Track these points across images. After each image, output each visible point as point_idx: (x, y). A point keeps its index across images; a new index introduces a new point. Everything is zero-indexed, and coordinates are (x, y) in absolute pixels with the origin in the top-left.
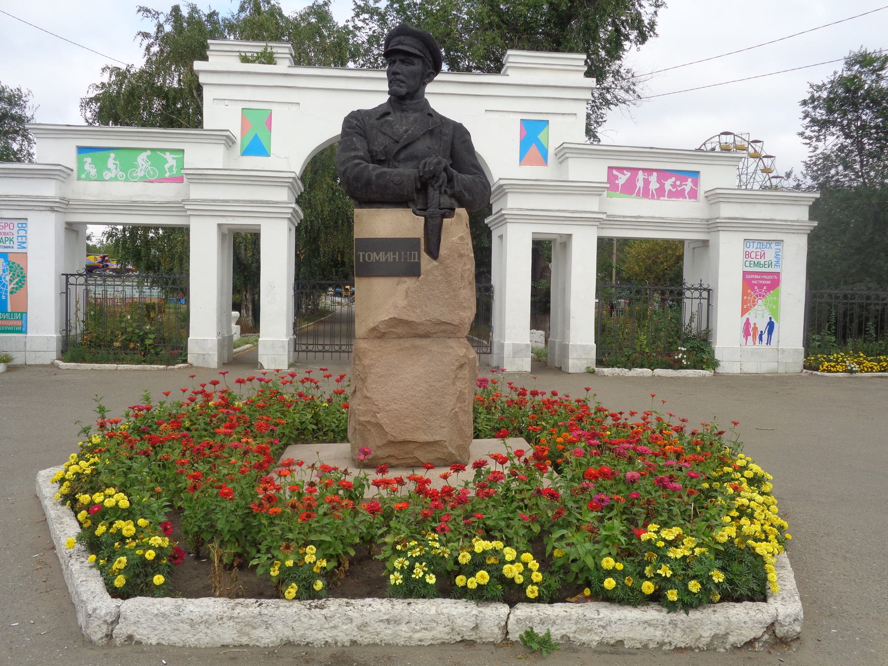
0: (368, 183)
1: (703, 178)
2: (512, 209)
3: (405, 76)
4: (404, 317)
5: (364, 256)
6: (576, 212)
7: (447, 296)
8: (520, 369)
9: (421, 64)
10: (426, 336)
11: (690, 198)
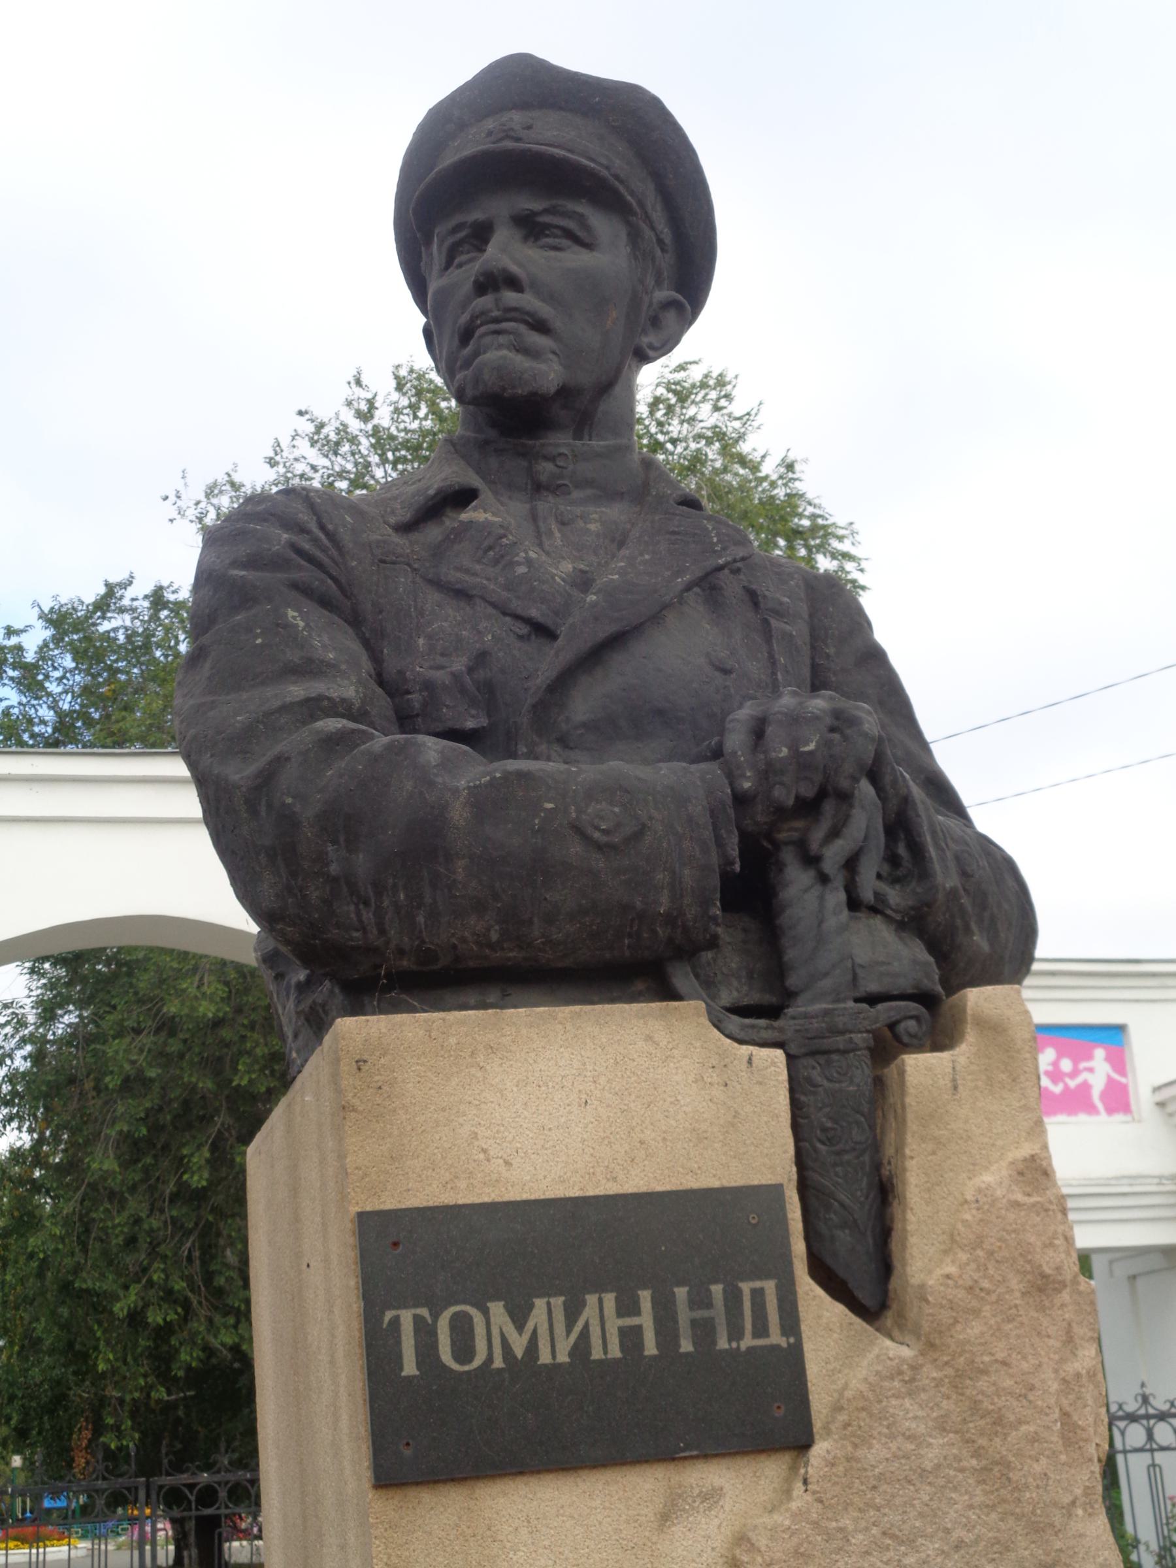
0: (425, 845)
1: (1139, 1044)
3: (551, 298)
9: (624, 250)
11: (1110, 1111)
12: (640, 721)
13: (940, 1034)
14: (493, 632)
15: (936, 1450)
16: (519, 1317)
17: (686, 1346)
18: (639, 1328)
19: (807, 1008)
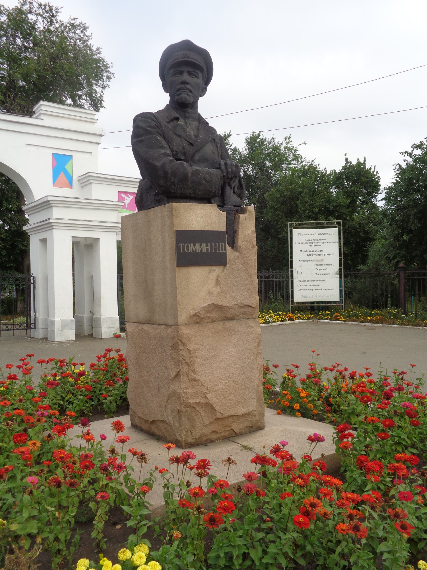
0: (185, 178)
2: (57, 219)
3: (192, 87)
4: (220, 303)
5: (183, 247)
6: (103, 222)
7: (246, 282)
8: (68, 339)
10: (232, 319)
12: (204, 160)
13: (243, 211)
14: (185, 144)
15: (240, 267)
16: (194, 246)
17: (213, 251)
18: (208, 249)
19: (228, 206)
